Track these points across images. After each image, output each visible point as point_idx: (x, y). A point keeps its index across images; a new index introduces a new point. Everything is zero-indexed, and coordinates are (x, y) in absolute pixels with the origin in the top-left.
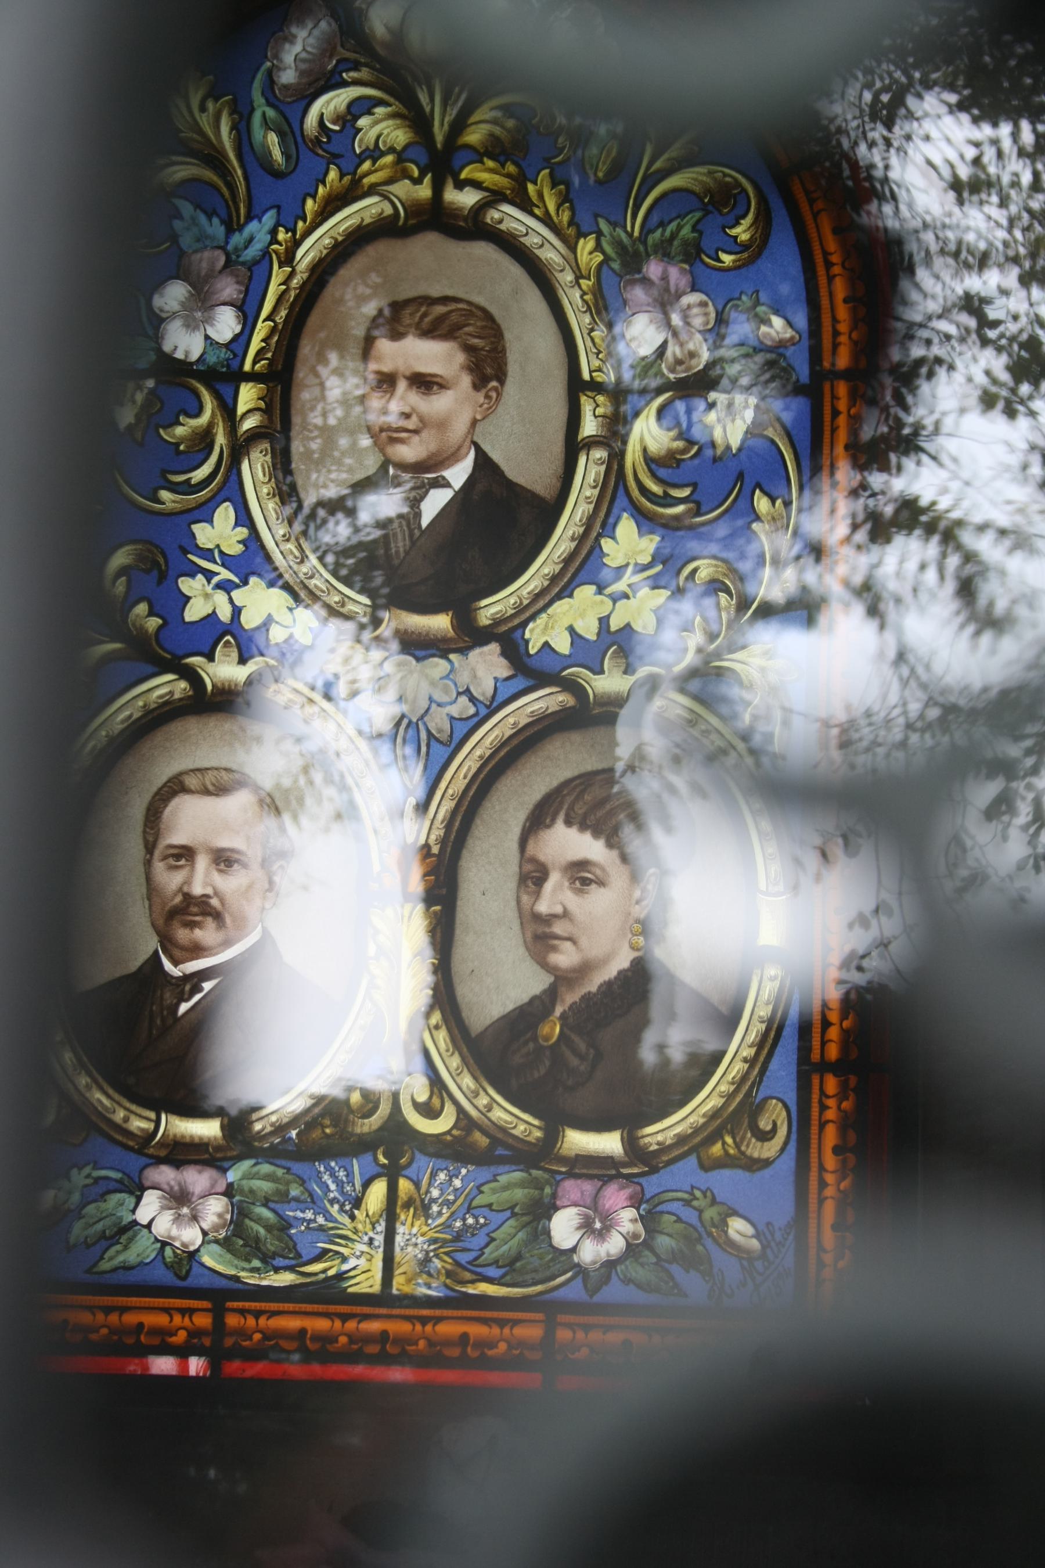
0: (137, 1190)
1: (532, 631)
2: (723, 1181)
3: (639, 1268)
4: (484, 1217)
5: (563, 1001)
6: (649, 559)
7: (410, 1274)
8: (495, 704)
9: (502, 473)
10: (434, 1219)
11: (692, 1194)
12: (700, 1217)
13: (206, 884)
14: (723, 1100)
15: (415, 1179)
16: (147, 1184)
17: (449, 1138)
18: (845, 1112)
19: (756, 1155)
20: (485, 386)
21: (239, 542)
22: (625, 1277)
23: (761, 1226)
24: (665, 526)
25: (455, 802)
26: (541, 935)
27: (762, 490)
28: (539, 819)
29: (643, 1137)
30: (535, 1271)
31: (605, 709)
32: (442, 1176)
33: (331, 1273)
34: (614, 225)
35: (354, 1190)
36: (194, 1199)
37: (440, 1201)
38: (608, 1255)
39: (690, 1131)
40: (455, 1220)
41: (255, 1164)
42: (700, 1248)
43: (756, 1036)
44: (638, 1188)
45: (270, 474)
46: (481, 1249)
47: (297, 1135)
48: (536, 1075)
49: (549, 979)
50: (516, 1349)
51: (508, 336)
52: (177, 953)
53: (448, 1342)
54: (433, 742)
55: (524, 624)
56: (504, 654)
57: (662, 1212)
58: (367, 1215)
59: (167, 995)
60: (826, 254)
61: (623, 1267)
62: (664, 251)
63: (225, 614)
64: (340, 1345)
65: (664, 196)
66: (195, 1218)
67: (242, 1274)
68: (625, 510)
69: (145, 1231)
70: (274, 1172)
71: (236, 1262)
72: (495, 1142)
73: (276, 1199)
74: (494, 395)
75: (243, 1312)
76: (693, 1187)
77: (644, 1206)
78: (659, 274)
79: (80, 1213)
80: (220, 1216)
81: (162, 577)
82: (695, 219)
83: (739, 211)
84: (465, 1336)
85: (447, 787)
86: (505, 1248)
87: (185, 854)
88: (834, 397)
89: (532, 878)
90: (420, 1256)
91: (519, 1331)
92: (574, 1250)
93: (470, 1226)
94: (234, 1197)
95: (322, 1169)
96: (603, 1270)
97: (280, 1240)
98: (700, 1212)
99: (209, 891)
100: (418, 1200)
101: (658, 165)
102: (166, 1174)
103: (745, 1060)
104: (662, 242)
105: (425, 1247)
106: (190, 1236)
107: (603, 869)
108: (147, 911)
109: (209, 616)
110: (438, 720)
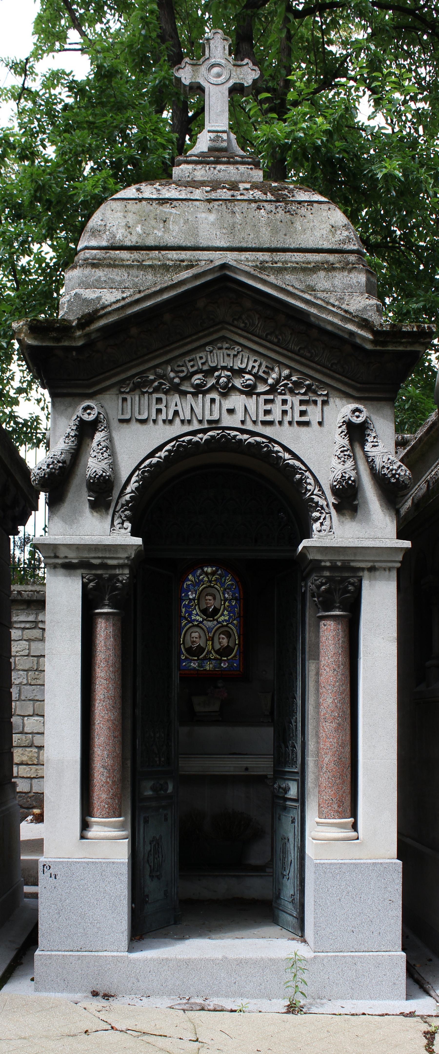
26: (220, 643)
87: (193, 638)
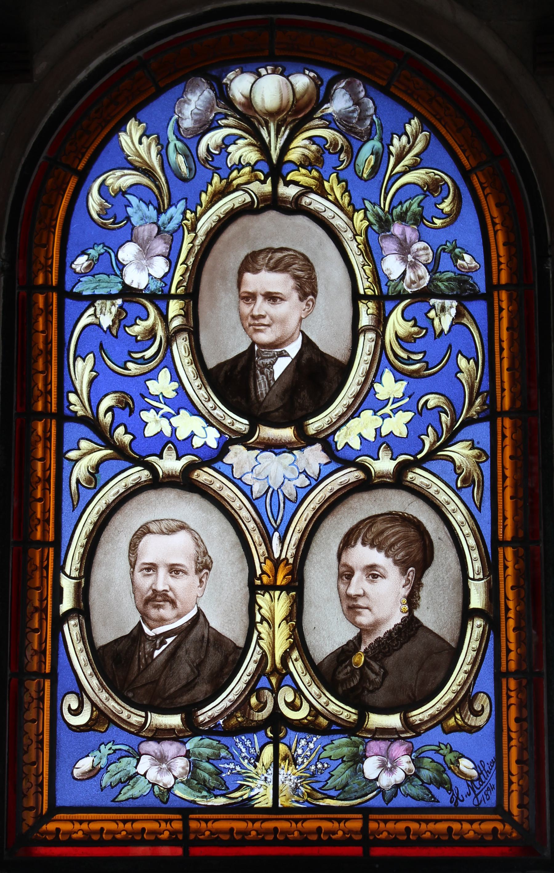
0: (138, 756)
1: (339, 436)
2: (456, 739)
3: (413, 788)
4: (327, 764)
5: (365, 643)
6: (402, 395)
7: (287, 796)
8: (320, 479)
9: (318, 347)
10: (299, 766)
11: (439, 746)
12: (444, 759)
13: (165, 584)
14: (454, 695)
15: (288, 744)
16: (142, 752)
17: (306, 721)
18: (521, 699)
19: (473, 724)
20: (306, 299)
21: (173, 390)
22: (405, 792)
23: (478, 763)
24: (409, 376)
25: (301, 534)
26: (351, 607)
27: (462, 355)
28: (347, 542)
29: (412, 717)
30: (356, 791)
31: (381, 479)
32: (303, 742)
33: (245, 797)
34: (374, 204)
35: (256, 752)
36: (168, 760)
37: (302, 756)
38: (395, 781)
39: (437, 712)
40: (311, 766)
41: (201, 739)
42: (445, 776)
43: (471, 659)
44: (411, 745)
45: (189, 352)
46: (326, 781)
47: (223, 722)
48: (352, 685)
49: (355, 631)
50: (348, 834)
51: (317, 269)
52: (151, 623)
53: (310, 832)
54: (287, 501)
55: (334, 433)
56: (324, 450)
57: (424, 757)
58: (263, 765)
59: (147, 646)
60: (492, 218)
61: (404, 787)
62: (402, 218)
63: (167, 432)
64: (252, 836)
65: (398, 190)
66: (170, 770)
67: (197, 799)
68: (386, 368)
69: (143, 777)
70: (212, 743)
71: (193, 793)
72: (331, 722)
73: (213, 758)
74: (311, 303)
75: (198, 820)
76: (439, 743)
77: (414, 754)
78: (400, 233)
79: (107, 769)
80: (183, 768)
81: (131, 412)
82: (419, 200)
83: (444, 194)
84: (319, 829)
85: (296, 526)
86: (340, 779)
87: (152, 568)
88: (500, 300)
89: (346, 575)
90: (293, 786)
91: (349, 825)
92: (377, 779)
93: (320, 769)
94: (190, 758)
95: (237, 741)
96: (393, 789)
97: (217, 780)
98: (444, 756)
99: (167, 588)
100: (290, 756)
101: (398, 169)
102: (151, 747)
103: (466, 672)
104: (401, 213)
105: (296, 781)
106: (167, 780)
107: (384, 569)
108: (133, 600)
109: (158, 433)
110: (289, 489)
